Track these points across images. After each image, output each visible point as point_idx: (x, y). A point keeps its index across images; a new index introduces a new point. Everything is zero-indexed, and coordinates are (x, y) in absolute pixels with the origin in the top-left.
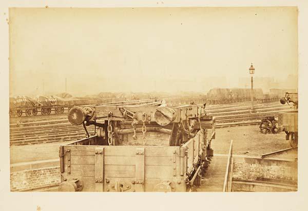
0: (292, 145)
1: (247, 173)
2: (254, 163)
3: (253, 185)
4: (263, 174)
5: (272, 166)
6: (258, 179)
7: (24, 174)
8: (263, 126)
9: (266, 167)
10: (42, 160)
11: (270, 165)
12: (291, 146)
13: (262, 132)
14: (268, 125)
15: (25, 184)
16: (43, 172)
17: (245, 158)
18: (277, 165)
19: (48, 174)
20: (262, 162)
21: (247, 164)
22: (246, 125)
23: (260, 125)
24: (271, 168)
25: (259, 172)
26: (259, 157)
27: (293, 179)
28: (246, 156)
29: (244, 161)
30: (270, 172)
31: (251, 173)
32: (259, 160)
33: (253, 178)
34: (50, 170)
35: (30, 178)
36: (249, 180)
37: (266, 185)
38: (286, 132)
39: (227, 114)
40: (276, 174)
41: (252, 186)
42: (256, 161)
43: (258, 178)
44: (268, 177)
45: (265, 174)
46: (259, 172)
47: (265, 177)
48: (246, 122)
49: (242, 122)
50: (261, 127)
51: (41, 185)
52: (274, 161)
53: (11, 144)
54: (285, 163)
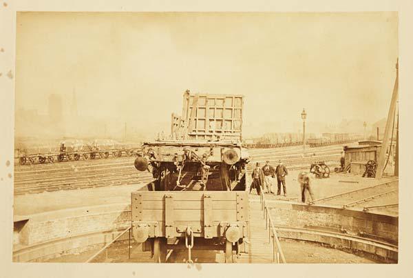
2: (302, 210)
3: (301, 233)
8: (313, 170)
9: (314, 215)
25: (306, 219)
33: (301, 225)
36: (296, 227)
37: (313, 233)
40: (325, 221)
46: (306, 219)
48: (298, 166)
51: (83, 232)
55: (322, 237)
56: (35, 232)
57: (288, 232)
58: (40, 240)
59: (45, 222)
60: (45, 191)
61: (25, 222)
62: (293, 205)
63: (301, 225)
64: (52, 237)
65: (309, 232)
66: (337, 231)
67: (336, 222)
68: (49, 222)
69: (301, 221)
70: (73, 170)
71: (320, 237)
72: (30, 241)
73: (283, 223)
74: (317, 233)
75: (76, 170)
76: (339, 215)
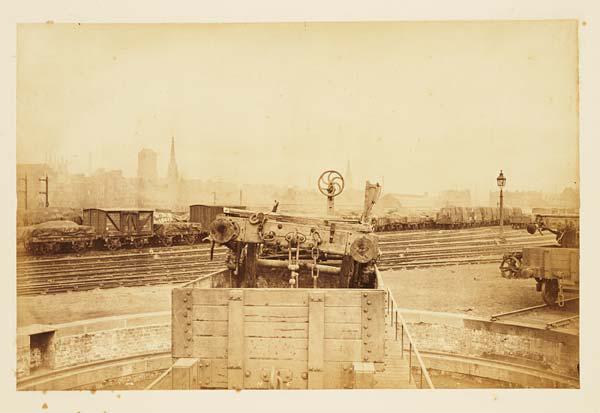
0: (548, 300)
2: (479, 329)
3: (476, 365)
6: (485, 355)
7: (115, 335)
8: (506, 265)
9: (499, 337)
10: (149, 312)
11: (506, 334)
12: (546, 301)
13: (504, 276)
15: (115, 350)
16: (144, 331)
17: (464, 320)
18: (517, 334)
19: (153, 334)
20: (492, 327)
22: (484, 262)
26: (488, 319)
27: (545, 359)
28: (465, 316)
29: (462, 323)
32: (488, 326)
33: (478, 352)
34: (156, 329)
35: (123, 342)
36: (470, 356)
37: (497, 366)
38: (537, 279)
40: (515, 348)
42: (483, 325)
43: (485, 353)
44: (503, 353)
47: (497, 352)
48: (485, 258)
49: (478, 258)
51: (141, 351)
53: (18, 295)
54: (531, 332)
55: (510, 373)
57: (456, 362)
58: (73, 362)
59: (80, 336)
62: (468, 322)
64: (91, 357)
65: (489, 365)
66: (535, 364)
67: (534, 350)
68: (86, 336)
69: (478, 346)
70: (151, 256)
71: (506, 374)
73: (448, 348)
74: (504, 367)
75: (156, 257)
76: (538, 340)
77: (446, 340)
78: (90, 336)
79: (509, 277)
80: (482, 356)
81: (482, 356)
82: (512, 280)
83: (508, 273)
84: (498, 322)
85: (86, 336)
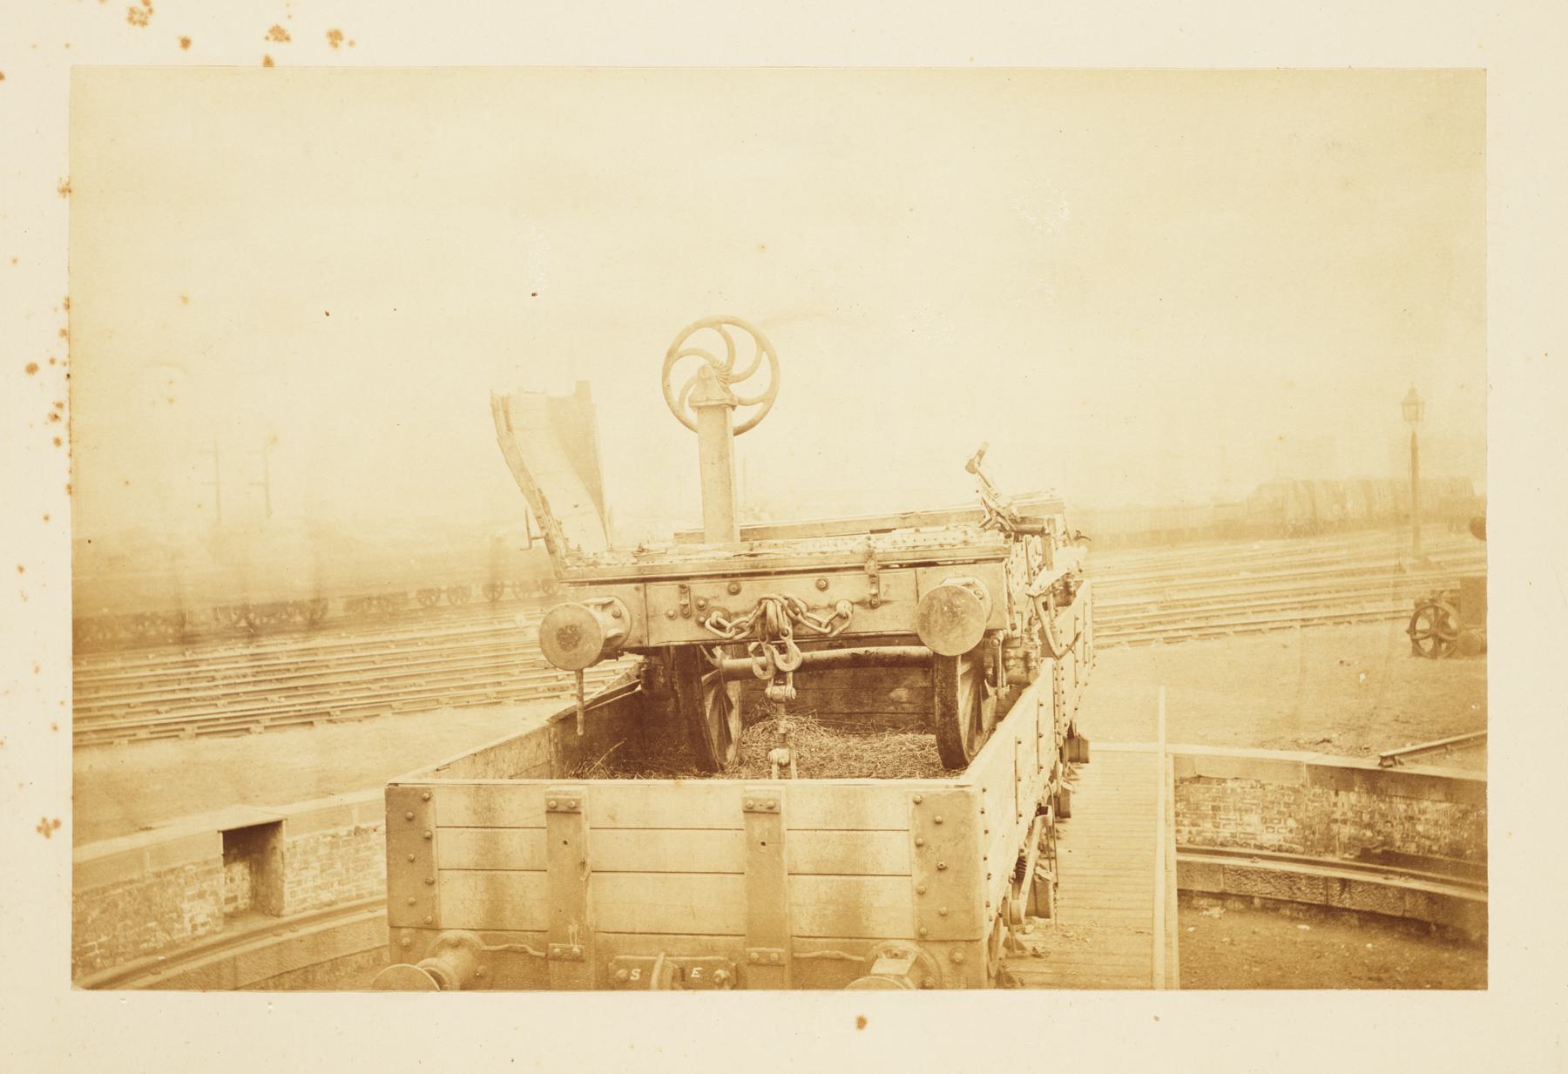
1: (1320, 828)
2: (1349, 788)
3: (1344, 883)
4: (1389, 835)
5: (1425, 804)
8: (1423, 624)
11: (1418, 799)
14: (1445, 624)
20: (1382, 784)
21: (1318, 790)
23: (1406, 624)
24: (1424, 812)
25: (1370, 826)
26: (1370, 763)
30: (1420, 828)
31: (1335, 827)
33: (1346, 847)
36: (1329, 858)
39: (1313, 577)
41: (1337, 887)
42: (1357, 779)
44: (1412, 849)
45: (1397, 836)
49: (1356, 609)
50: (1412, 630)
52: (1434, 781)
56: (306, 866)
57: (1290, 876)
58: (326, 896)
59: (343, 831)
60: (388, 713)
61: (269, 830)
62: (1314, 769)
63: (1346, 847)
65: (1379, 879)
68: (357, 831)
69: (1346, 832)
71: (1422, 902)
72: (287, 898)
73: (1269, 838)
77: (1264, 821)
78: (366, 831)
79: (1434, 655)
80: (1359, 858)
81: (1359, 858)
82: (1440, 663)
83: (1428, 645)
84: (1398, 769)
85: (357, 831)
